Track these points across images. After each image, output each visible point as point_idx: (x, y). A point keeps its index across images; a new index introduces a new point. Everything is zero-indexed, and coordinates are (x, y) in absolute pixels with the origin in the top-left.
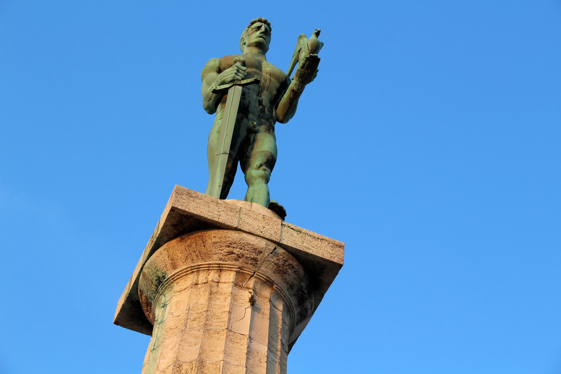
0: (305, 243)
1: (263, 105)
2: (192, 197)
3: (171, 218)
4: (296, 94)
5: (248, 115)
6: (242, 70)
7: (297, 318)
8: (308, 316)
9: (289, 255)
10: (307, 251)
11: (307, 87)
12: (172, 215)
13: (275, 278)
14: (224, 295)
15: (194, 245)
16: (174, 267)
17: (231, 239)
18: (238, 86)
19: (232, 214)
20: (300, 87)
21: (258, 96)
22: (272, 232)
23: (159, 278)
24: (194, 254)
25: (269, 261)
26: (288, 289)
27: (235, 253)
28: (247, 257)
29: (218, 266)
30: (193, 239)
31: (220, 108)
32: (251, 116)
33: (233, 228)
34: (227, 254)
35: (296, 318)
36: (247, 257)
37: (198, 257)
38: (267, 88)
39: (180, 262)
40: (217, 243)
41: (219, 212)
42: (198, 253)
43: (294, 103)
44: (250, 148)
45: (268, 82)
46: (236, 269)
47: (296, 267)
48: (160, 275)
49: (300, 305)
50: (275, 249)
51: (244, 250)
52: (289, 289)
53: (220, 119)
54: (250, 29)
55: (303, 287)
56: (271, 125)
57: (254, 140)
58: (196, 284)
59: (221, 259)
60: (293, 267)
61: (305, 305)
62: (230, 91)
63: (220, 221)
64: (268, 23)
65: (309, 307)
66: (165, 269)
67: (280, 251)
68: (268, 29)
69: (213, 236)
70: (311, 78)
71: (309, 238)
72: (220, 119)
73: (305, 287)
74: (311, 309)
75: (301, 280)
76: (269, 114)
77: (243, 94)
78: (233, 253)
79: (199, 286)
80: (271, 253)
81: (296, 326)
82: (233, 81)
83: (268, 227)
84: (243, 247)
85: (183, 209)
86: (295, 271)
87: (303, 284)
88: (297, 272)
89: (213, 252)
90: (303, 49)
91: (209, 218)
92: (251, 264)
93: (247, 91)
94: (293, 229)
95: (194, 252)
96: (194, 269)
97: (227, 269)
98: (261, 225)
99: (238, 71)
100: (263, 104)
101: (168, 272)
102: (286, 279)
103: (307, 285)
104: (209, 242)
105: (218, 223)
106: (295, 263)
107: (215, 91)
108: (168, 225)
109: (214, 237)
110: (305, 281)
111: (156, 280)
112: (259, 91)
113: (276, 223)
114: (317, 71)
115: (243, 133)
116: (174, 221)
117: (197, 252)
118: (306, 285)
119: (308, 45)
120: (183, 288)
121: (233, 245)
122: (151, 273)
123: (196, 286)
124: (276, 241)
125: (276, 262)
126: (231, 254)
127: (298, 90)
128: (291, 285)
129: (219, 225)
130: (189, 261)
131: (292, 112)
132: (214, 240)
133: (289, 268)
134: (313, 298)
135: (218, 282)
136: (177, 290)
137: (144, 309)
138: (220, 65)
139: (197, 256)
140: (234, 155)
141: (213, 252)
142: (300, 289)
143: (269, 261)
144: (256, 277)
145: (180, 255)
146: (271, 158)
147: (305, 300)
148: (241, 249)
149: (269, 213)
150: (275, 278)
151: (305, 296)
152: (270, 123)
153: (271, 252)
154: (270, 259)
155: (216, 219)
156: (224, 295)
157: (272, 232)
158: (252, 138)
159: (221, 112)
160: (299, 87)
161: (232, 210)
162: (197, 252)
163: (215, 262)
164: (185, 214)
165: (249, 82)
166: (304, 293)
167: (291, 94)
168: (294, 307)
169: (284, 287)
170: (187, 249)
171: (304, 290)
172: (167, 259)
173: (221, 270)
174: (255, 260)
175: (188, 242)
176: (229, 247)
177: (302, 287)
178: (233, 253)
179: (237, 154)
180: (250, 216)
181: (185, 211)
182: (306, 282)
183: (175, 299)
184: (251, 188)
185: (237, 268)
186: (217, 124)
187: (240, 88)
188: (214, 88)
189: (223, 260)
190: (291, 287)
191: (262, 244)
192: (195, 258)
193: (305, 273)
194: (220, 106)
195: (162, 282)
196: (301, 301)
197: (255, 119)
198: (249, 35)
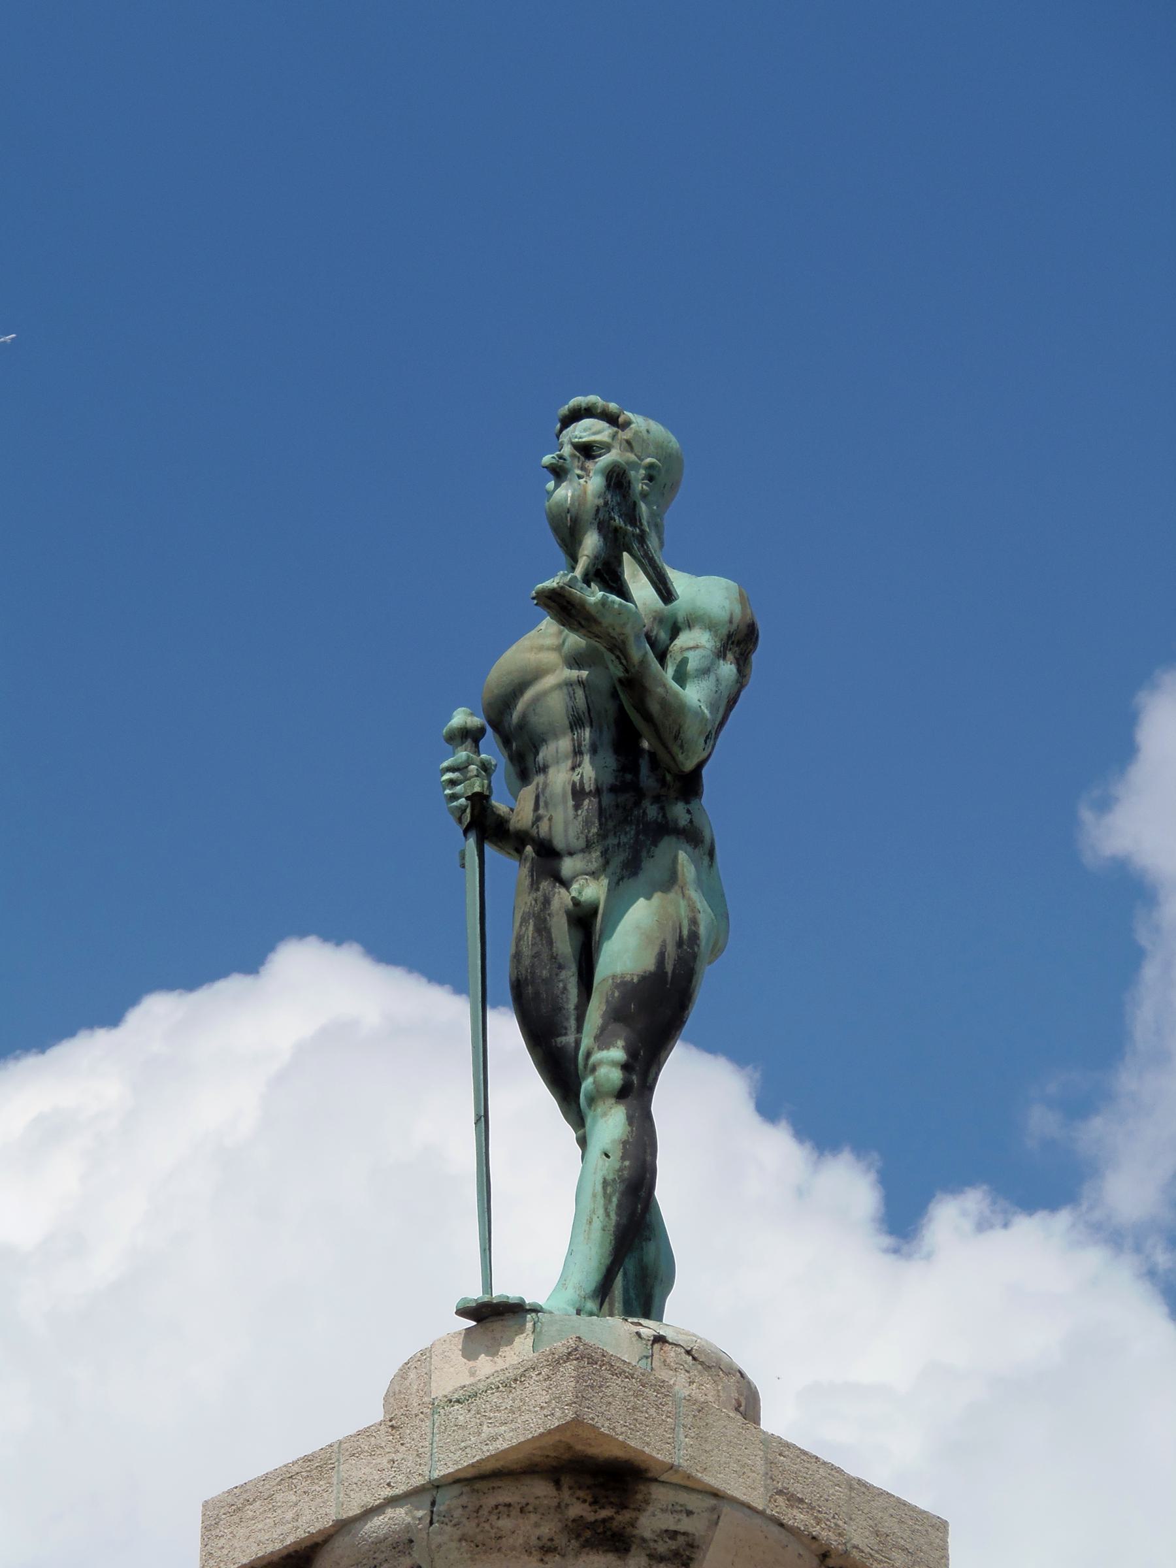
9: (477, 1486)
20: (624, 662)
25: (440, 1546)
38: (586, 714)
43: (654, 708)
52: (546, 1559)
55: (582, 1517)
60: (509, 1505)
64: (585, 409)
73: (589, 1509)
74: (689, 1513)
80: (431, 1523)
87: (577, 1509)
88: (527, 1504)
91: (278, 1546)
102: (513, 1549)
103: (589, 1499)
106: (508, 1494)
110: (575, 1500)
112: (574, 749)
118: (587, 1504)
125: (458, 1533)
127: (626, 670)
131: (680, 727)
133: (499, 1518)
143: (440, 1546)
153: (428, 1521)
154: (439, 1539)
171: (591, 1517)
177: (579, 1520)
182: (578, 1499)
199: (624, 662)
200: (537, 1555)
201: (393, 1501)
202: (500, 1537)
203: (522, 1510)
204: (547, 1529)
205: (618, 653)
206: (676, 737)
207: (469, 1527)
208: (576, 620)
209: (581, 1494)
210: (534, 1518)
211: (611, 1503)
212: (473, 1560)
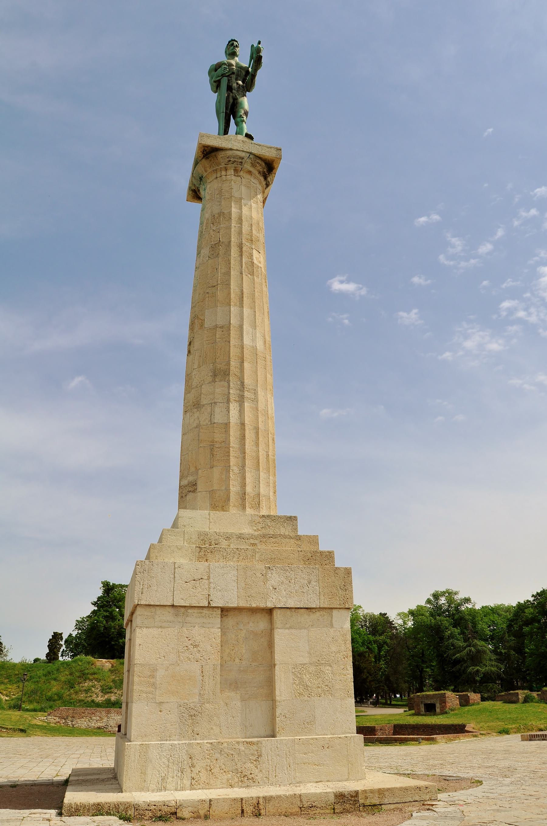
4: (254, 76)
5: (232, 91)
10: (265, 154)
11: (259, 71)
13: (251, 169)
15: (213, 160)
16: (206, 171)
17: (229, 154)
18: (225, 77)
19: (228, 142)
21: (236, 80)
22: (247, 148)
24: (213, 164)
32: (234, 91)
35: (265, 186)
39: (208, 169)
44: (235, 107)
45: (240, 72)
48: (201, 176)
50: (250, 155)
59: (225, 165)
62: (222, 81)
65: (270, 180)
67: (251, 156)
69: (221, 155)
71: (265, 148)
75: (264, 168)
77: (229, 80)
78: (230, 161)
82: (223, 75)
83: (245, 146)
85: (204, 143)
87: (265, 170)
90: (254, 52)
93: (230, 78)
98: (241, 145)
99: (224, 69)
101: (204, 174)
105: (221, 147)
106: (259, 161)
107: (215, 82)
115: (231, 100)
116: (202, 150)
120: (211, 180)
125: (251, 162)
128: (259, 172)
129: (221, 148)
132: (221, 156)
134: (271, 176)
137: (198, 193)
138: (216, 67)
139: (215, 165)
142: (264, 172)
144: (243, 171)
145: (208, 166)
149: (246, 139)
150: (251, 169)
155: (221, 146)
157: (247, 148)
158: (236, 102)
162: (215, 163)
163: (223, 166)
166: (267, 174)
169: (257, 173)
173: (226, 170)
174: (241, 162)
175: (210, 159)
177: (265, 172)
178: (230, 161)
181: (205, 144)
183: (208, 187)
184: (238, 128)
187: (226, 78)
189: (227, 165)
190: (260, 173)
191: (243, 154)
194: (218, 89)
196: (265, 178)
197: (236, 92)
198: (228, 49)
200: (258, 172)
201: (243, 151)
203: (261, 165)
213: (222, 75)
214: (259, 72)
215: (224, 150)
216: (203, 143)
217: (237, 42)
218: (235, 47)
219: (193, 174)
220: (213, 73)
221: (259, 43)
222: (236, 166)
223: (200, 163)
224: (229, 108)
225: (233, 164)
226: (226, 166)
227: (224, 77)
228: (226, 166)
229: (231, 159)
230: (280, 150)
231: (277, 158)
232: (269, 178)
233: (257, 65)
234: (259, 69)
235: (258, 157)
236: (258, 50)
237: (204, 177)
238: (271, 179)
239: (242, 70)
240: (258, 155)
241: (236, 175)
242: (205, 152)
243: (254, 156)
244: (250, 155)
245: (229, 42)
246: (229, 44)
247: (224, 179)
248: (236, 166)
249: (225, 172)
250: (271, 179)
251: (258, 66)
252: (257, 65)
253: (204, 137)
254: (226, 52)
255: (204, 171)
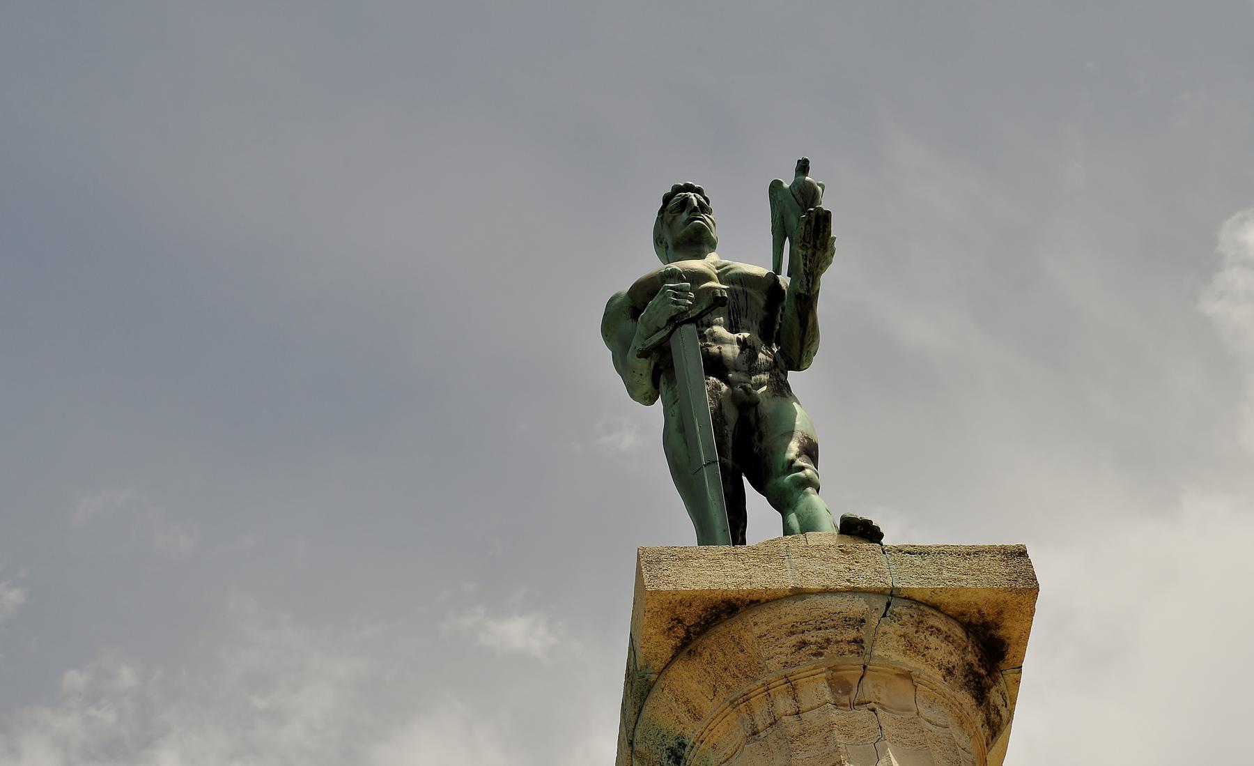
0: (944, 572)
1: (749, 347)
2: (680, 559)
3: (652, 617)
4: (806, 301)
6: (681, 290)
7: (984, 732)
8: (1004, 721)
10: (957, 584)
12: (652, 611)
13: (912, 663)
14: (819, 733)
23: (672, 751)
25: (885, 633)
26: (944, 678)
27: (811, 644)
28: (837, 642)
29: (785, 680)
30: (711, 644)
31: (664, 383)
33: (788, 593)
34: (794, 648)
35: (984, 732)
36: (839, 642)
37: (737, 677)
38: (745, 310)
40: (765, 635)
41: (746, 570)
42: (734, 669)
43: (810, 322)
44: (756, 438)
45: (742, 298)
46: (824, 675)
47: (944, 628)
48: (673, 743)
49: (980, 704)
50: (888, 605)
51: (827, 628)
53: (674, 403)
54: (666, 214)
55: (972, 664)
56: (782, 381)
57: (758, 420)
58: (754, 734)
60: (939, 630)
61: (991, 701)
62: (675, 344)
63: (757, 586)
66: (679, 728)
68: (702, 200)
70: (826, 258)
72: (674, 403)
73: (977, 662)
74: (1006, 706)
76: (768, 359)
78: (804, 644)
79: (762, 734)
80: (884, 615)
81: (989, 751)
82: (676, 321)
83: (857, 567)
84: (822, 623)
85: (671, 587)
86: (946, 636)
87: (970, 658)
88: (950, 636)
89: (765, 655)
92: (852, 652)
94: (909, 553)
95: (726, 669)
96: (738, 705)
97: (808, 679)
98: (841, 567)
100: (749, 344)
101: (686, 732)
103: (979, 657)
104: (749, 637)
105: (749, 592)
106: (937, 621)
108: (651, 634)
109: (756, 624)
111: (669, 757)
112: (731, 322)
113: (870, 553)
114: (834, 239)
117: (733, 669)
119: (793, 196)
121: (801, 628)
122: (654, 748)
123: (756, 737)
124: (885, 589)
126: (803, 647)
127: (808, 291)
129: (755, 598)
130: (721, 692)
131: (813, 341)
132: (757, 631)
133: (931, 635)
135: (798, 713)
136: (720, 760)
139: (734, 676)
140: (729, 461)
141: (765, 655)
142: (969, 670)
143: (885, 633)
146: (806, 441)
147: (987, 691)
148: (820, 629)
150: (912, 663)
151: (984, 682)
152: (777, 379)
154: (886, 628)
156: (819, 733)
158: (752, 418)
159: (670, 388)
160: (808, 285)
161: (769, 558)
162: (733, 669)
164: (678, 598)
165: (704, 308)
166: (983, 677)
167: (799, 305)
168: (970, 712)
170: (708, 669)
171: (976, 669)
172: (675, 705)
174: (858, 642)
175: (706, 655)
176: (792, 633)
177: (970, 665)
178: (804, 644)
179: (733, 460)
180: (813, 557)
181: (677, 592)
185: (825, 672)
186: (673, 416)
188: (639, 347)
191: (858, 606)
192: (730, 682)
193: (967, 634)
194: (663, 379)
195: (681, 757)
196: (980, 694)
198: (670, 225)
199: (810, 285)
201: (855, 591)
202: (927, 648)
204: (955, 659)
205: (811, 279)
206: (809, 345)
207: (911, 630)
208: (814, 241)
209: (976, 648)
210: (951, 647)
211: (986, 667)
212: (905, 653)
213: (672, 320)
214: (829, 282)
215: (767, 601)
216: (664, 588)
217: (699, 191)
218: (695, 210)
219: (631, 743)
220: (627, 324)
221: (803, 167)
222: (838, 660)
223: (661, 683)
224: (730, 444)
225: (821, 654)
226: (788, 671)
227: (681, 324)
228: (788, 671)
229: (808, 637)
230: (1022, 553)
231: (1019, 592)
232: (993, 691)
233: (813, 254)
234: (823, 269)
235: (927, 604)
236: (805, 195)
237: (689, 743)
238: (1003, 695)
239: (749, 290)
240: (927, 596)
241: (845, 699)
242: (681, 632)
243: (908, 603)
244: (888, 605)
245: (667, 199)
246: (670, 206)
247: (794, 730)
248: (838, 660)
249: (790, 701)
250: (1003, 695)
251: (819, 254)
252: (813, 254)
253: (664, 565)
254: (659, 241)
255: (685, 718)
